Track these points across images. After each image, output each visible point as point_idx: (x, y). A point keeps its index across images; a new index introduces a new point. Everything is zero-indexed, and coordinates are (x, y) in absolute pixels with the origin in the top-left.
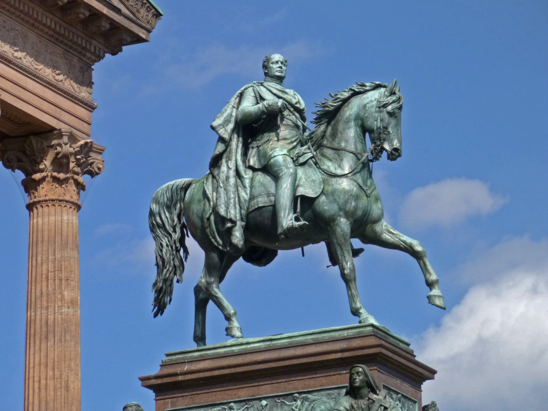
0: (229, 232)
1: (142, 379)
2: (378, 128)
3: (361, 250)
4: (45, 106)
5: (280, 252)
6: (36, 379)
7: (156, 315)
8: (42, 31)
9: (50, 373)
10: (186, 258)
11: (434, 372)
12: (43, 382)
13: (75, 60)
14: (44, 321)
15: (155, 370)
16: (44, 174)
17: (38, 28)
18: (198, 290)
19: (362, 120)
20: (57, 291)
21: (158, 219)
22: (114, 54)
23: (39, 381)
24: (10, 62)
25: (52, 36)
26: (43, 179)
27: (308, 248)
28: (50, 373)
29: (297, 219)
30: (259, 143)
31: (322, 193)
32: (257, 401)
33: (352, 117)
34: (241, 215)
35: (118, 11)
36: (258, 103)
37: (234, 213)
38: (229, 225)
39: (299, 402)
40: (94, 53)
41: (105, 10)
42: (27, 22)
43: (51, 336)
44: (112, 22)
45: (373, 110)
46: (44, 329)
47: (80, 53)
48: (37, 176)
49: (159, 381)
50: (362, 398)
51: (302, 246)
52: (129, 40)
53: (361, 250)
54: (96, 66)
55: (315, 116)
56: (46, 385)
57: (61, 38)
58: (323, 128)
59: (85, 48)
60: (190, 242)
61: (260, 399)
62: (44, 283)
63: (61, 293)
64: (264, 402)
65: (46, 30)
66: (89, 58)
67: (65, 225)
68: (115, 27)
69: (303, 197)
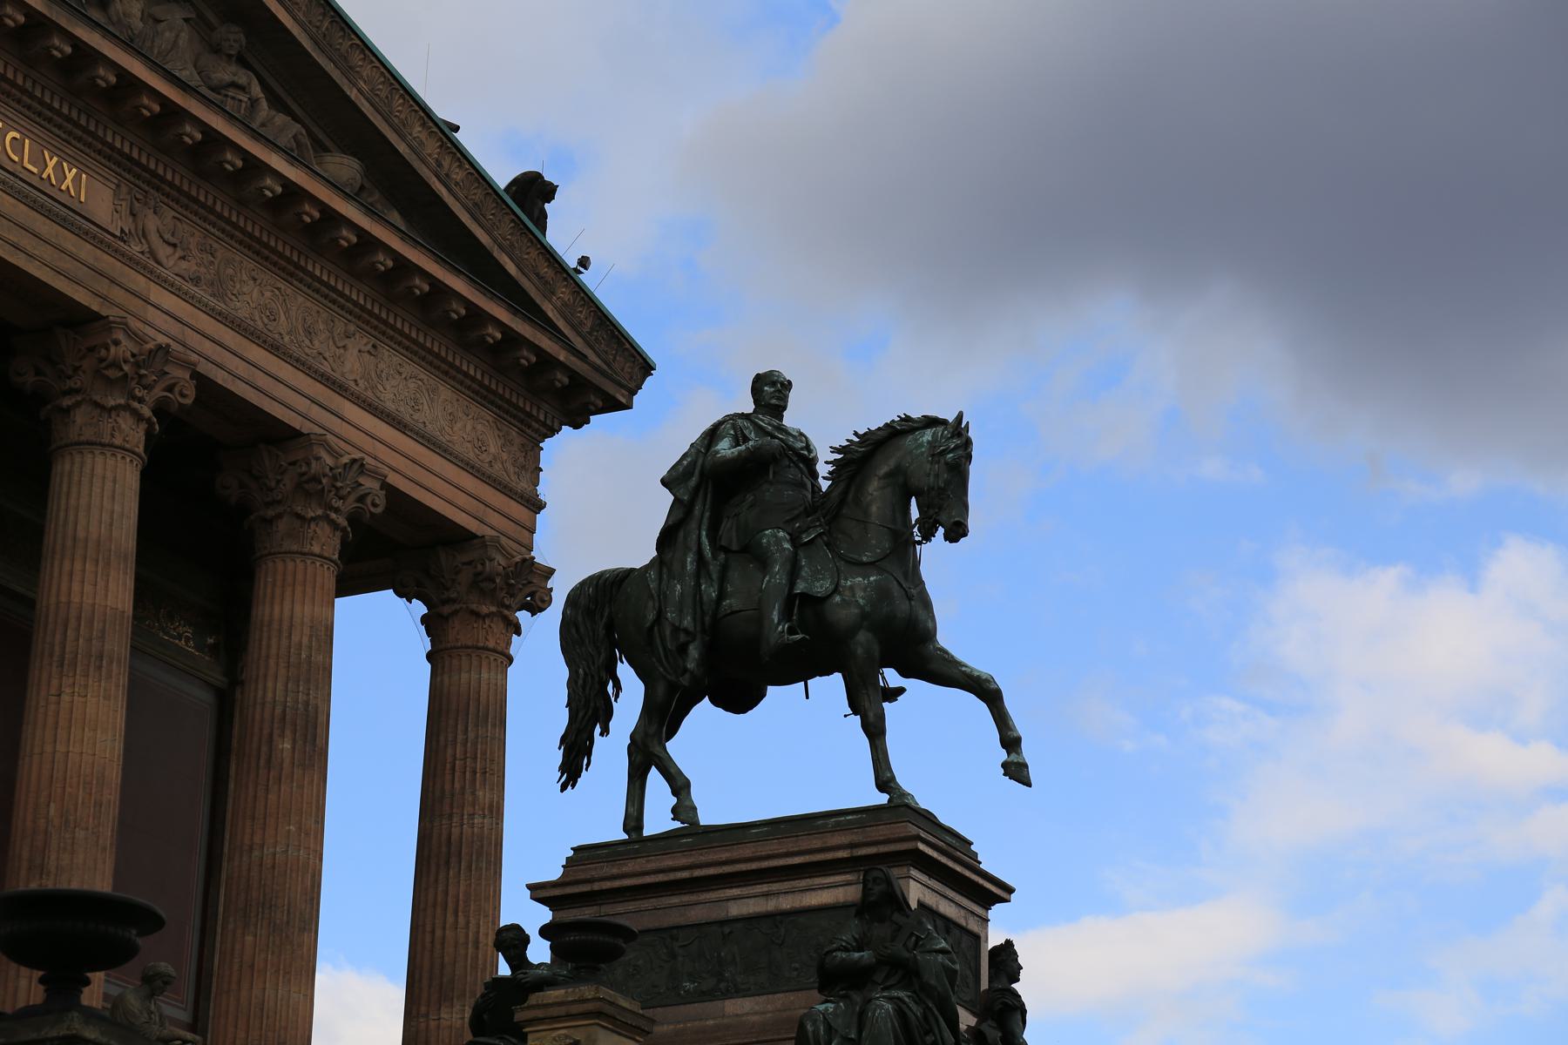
0: (683, 650)
1: (529, 887)
2: (931, 489)
3: (901, 691)
4: (462, 499)
5: (771, 689)
6: (428, 928)
7: (563, 788)
8: (461, 383)
9: (450, 919)
10: (617, 696)
11: (1010, 890)
12: (438, 933)
13: (514, 433)
14: (444, 837)
15: (554, 873)
16: (457, 606)
17: (454, 378)
18: (631, 750)
20: (468, 791)
22: (577, 426)
23: (433, 932)
24: (405, 426)
25: (477, 393)
26: (455, 613)
27: (816, 683)
28: (450, 919)
29: (791, 631)
31: (835, 591)
34: (703, 623)
35: (583, 357)
36: (738, 445)
38: (683, 638)
40: (544, 424)
41: (562, 356)
42: (438, 368)
43: (453, 860)
44: (573, 374)
46: (444, 849)
47: (522, 422)
48: (446, 610)
49: (557, 892)
51: (805, 678)
52: (600, 404)
53: (901, 691)
54: (547, 444)
55: (830, 468)
56: (444, 937)
57: (492, 397)
58: (842, 486)
59: (529, 415)
60: (625, 671)
62: (448, 777)
63: (473, 793)
64: (727, 930)
65: (468, 382)
66: (536, 431)
67: (484, 687)
68: (578, 384)
69: (806, 598)
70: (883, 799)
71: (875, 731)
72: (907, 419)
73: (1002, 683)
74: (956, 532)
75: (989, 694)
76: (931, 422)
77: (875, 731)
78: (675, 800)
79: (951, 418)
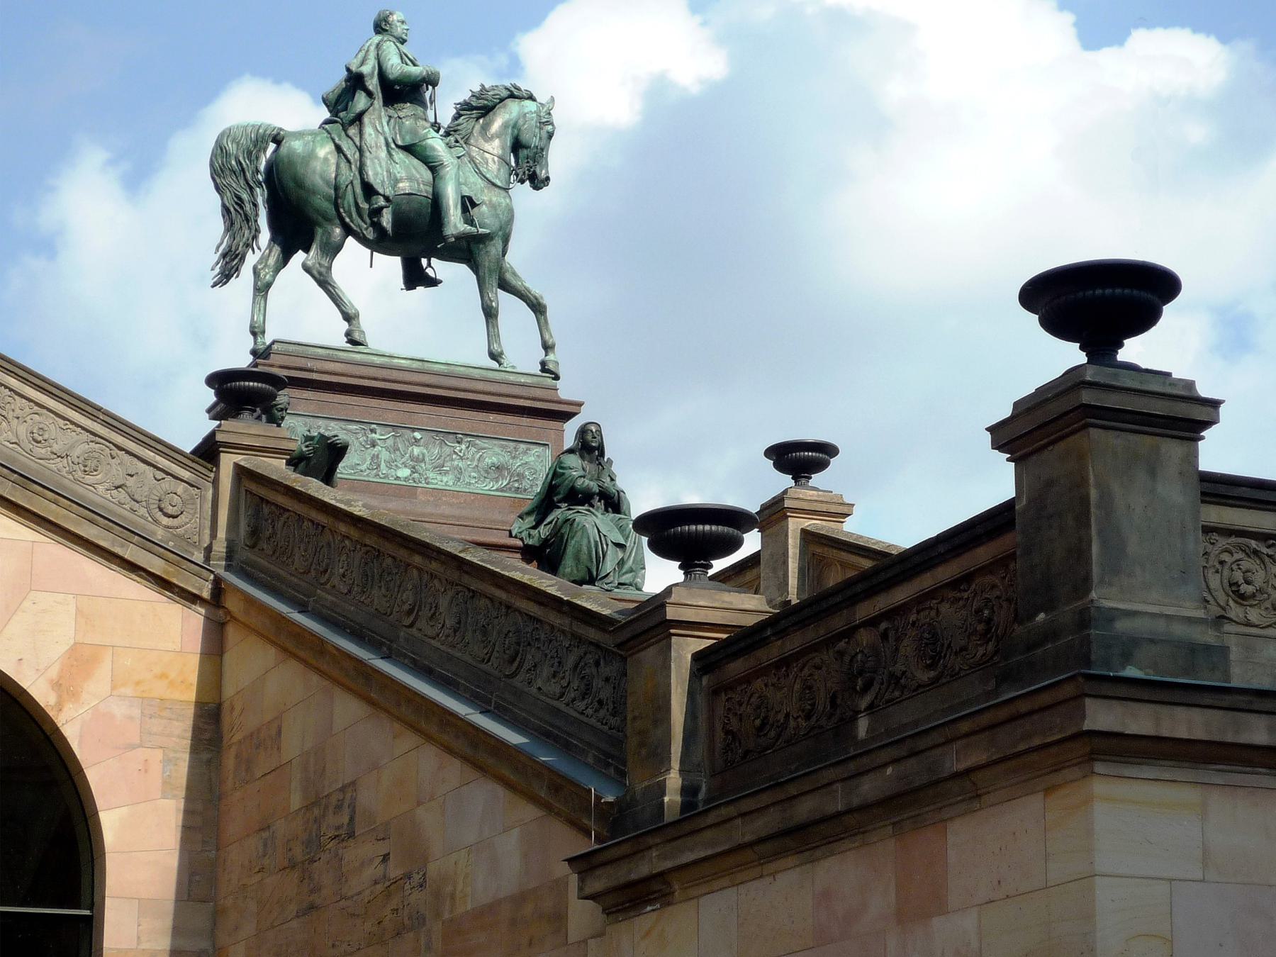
0: (377, 212)
19: (519, 130)
21: (233, 162)
30: (401, 114)
32: (408, 432)
33: (512, 123)
37: (389, 192)
38: (382, 202)
39: (463, 447)
45: (533, 123)
50: (591, 462)
61: (414, 430)
64: (417, 435)
69: (470, 199)
70: (495, 365)
71: (490, 314)
72: (519, 89)
73: (546, 301)
74: (538, 182)
75: (538, 308)
76: (531, 98)
77: (490, 314)
78: (345, 326)
79: (542, 97)
